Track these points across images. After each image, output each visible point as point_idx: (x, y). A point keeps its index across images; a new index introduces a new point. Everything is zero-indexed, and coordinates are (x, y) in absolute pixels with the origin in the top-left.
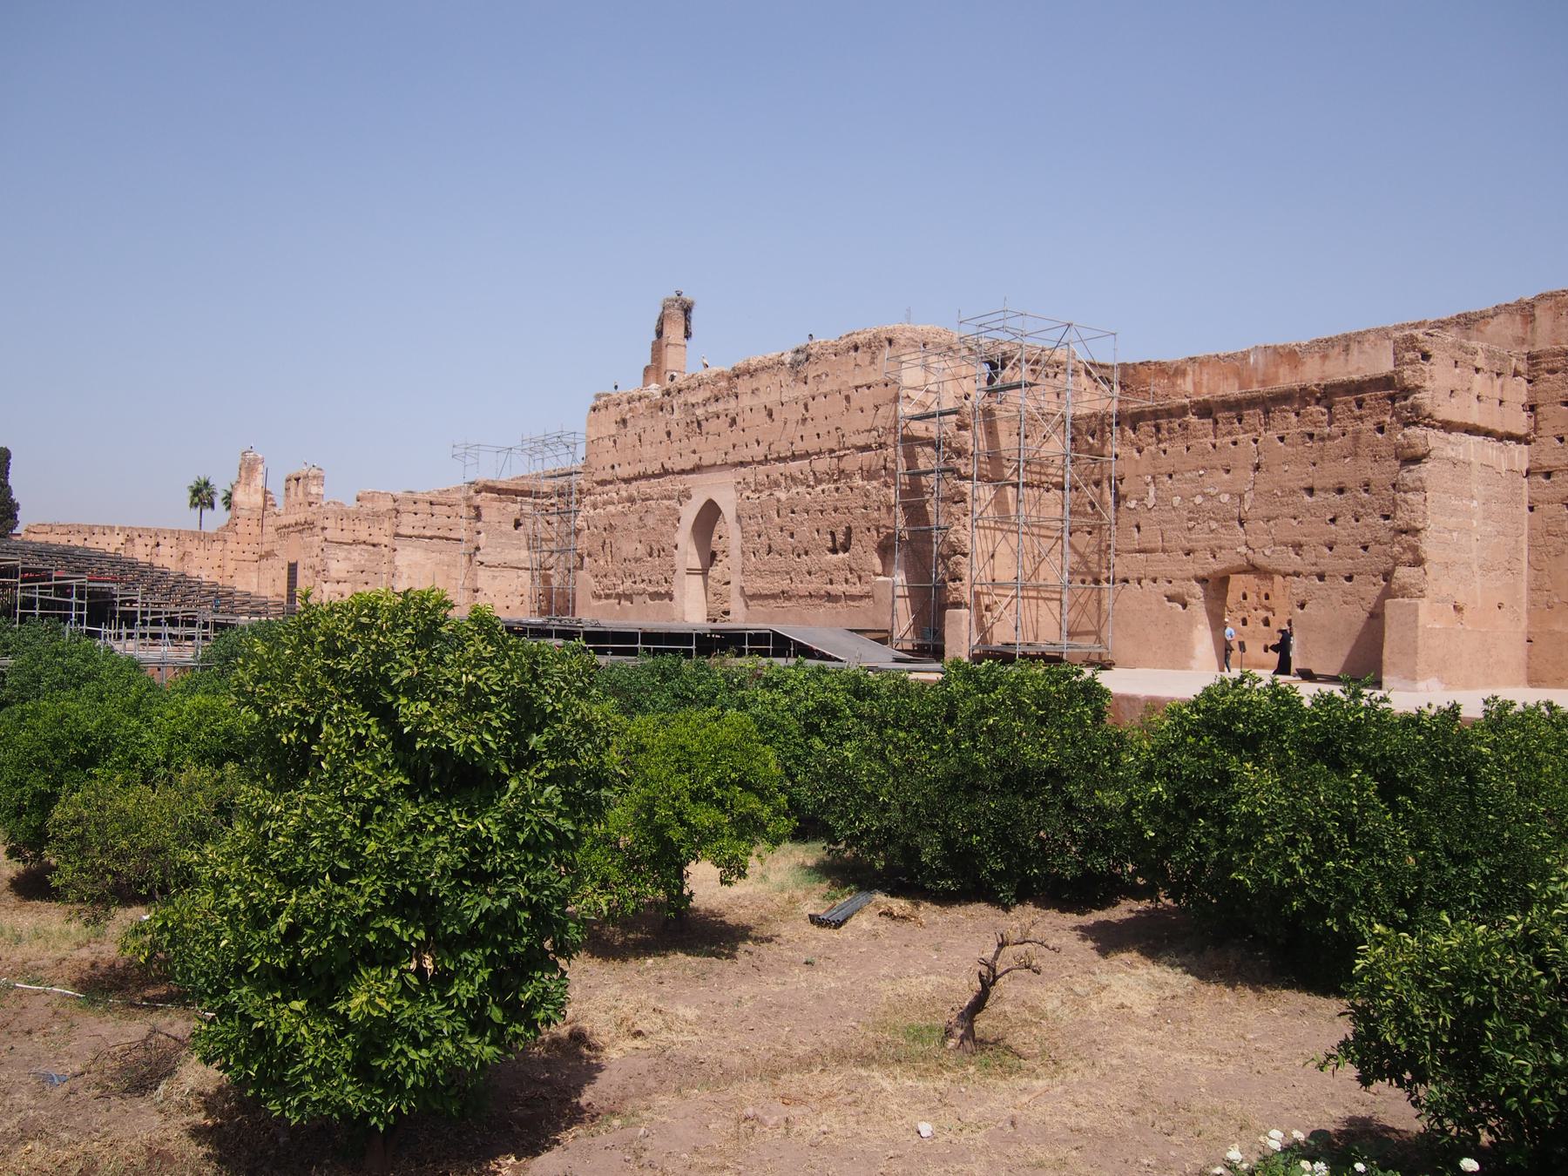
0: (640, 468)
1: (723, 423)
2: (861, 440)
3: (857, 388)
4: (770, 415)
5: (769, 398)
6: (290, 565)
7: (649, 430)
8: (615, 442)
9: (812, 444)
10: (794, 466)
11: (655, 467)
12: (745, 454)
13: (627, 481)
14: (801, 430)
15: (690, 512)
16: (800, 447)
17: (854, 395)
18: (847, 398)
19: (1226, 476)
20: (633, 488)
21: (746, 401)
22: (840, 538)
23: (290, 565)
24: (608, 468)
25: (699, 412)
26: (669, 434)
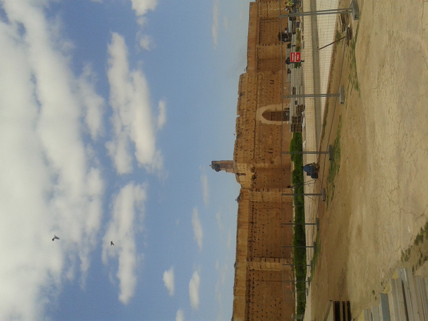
0: (253, 139)
2: (257, 79)
3: (248, 81)
5: (246, 100)
8: (245, 151)
10: (258, 94)
12: (255, 105)
13: (255, 144)
15: (264, 121)
16: (256, 93)
18: (249, 83)
19: (268, 39)
20: (257, 143)
22: (272, 82)
24: (251, 153)
25: (244, 120)
26: (247, 130)
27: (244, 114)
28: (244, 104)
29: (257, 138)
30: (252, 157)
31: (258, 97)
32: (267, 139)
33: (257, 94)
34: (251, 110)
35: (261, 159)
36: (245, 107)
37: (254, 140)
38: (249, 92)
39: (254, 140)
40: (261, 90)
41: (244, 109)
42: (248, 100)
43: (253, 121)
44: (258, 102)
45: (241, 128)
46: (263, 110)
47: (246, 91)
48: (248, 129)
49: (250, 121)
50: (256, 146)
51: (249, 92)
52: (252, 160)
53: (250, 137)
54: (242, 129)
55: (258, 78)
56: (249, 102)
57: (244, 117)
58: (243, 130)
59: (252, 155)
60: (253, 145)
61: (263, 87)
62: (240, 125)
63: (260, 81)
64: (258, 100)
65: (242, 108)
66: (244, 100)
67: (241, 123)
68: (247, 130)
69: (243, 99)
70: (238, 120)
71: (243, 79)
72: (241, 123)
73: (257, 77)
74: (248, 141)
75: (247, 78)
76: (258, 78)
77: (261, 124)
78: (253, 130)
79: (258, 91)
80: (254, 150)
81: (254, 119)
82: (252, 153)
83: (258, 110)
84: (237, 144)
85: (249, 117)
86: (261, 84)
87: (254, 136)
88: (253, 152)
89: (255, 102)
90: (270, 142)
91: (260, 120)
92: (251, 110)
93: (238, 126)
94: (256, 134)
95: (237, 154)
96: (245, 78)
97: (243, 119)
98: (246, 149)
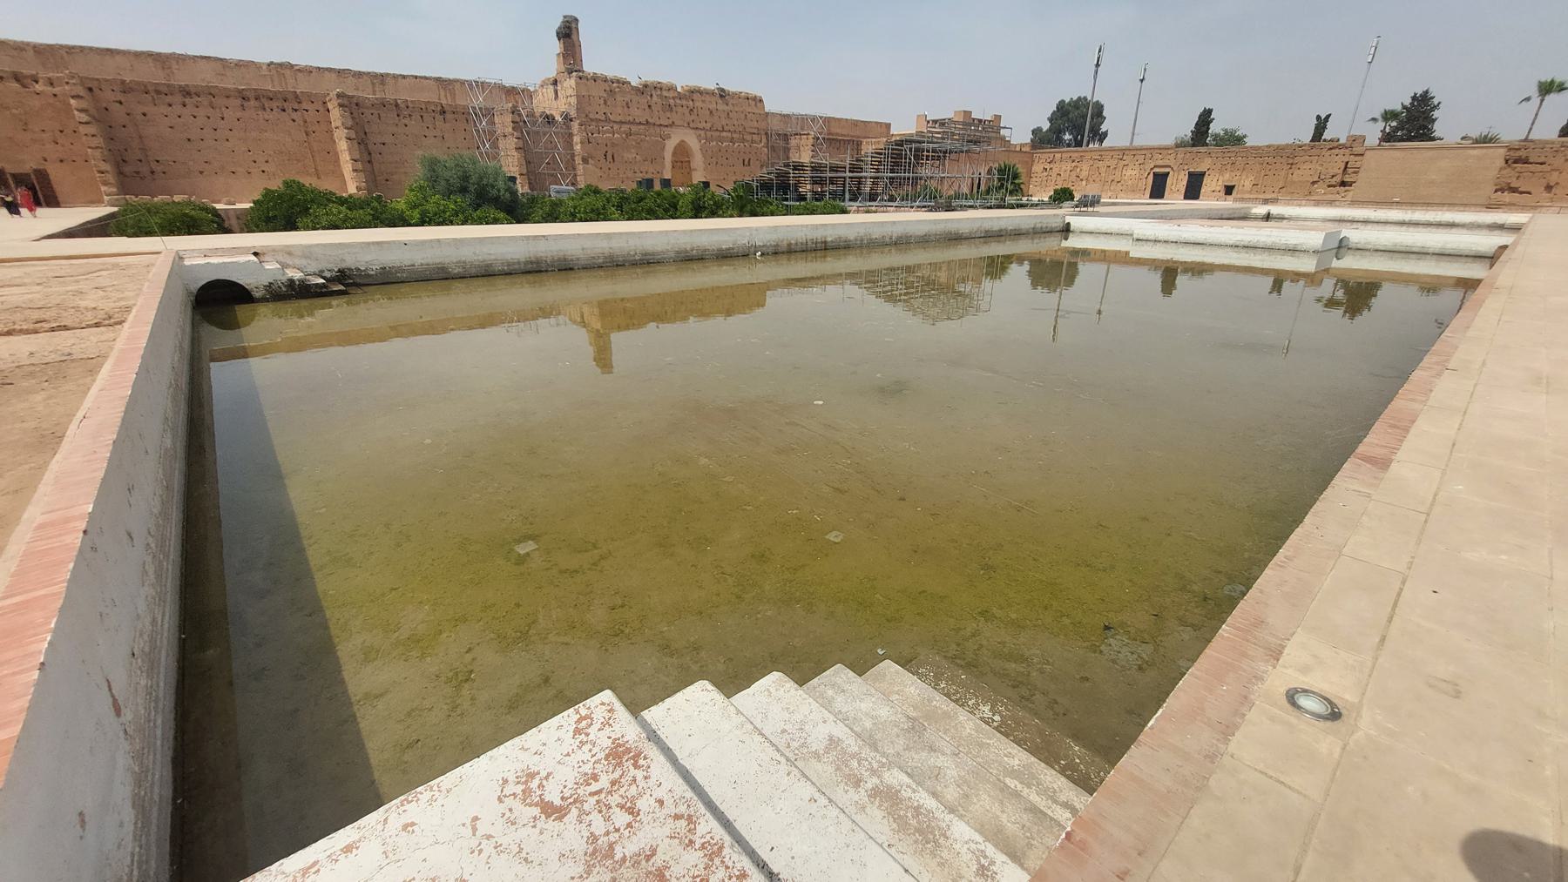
0: (631, 119)
1: (687, 112)
4: (711, 112)
5: (713, 106)
7: (634, 101)
10: (724, 134)
12: (700, 126)
13: (621, 122)
15: (671, 145)
20: (625, 128)
22: (746, 162)
27: (684, 102)
28: (703, 101)
29: (634, 128)
30: (591, 116)
31: (718, 133)
32: (633, 151)
33: (723, 131)
34: (693, 117)
35: (590, 134)
36: (699, 104)
37: (630, 123)
38: (728, 114)
39: (630, 123)
40: (732, 140)
41: (693, 100)
42: (711, 112)
44: (709, 133)
45: (653, 92)
46: (693, 143)
47: (730, 107)
48: (653, 108)
49: (668, 114)
50: (616, 127)
51: (728, 114)
52: (587, 116)
53: (638, 114)
54: (651, 95)
55: (754, 134)
56: (709, 112)
57: (678, 101)
58: (649, 98)
59: (597, 116)
60: (618, 119)
61: (737, 144)
62: (659, 93)
63: (748, 137)
65: (696, 96)
67: (665, 93)
68: (649, 106)
69: (713, 99)
70: (672, 88)
74: (626, 108)
75: (756, 111)
76: (754, 134)
77: (665, 138)
78: (650, 120)
79: (729, 134)
80: (607, 120)
81: (673, 123)
83: (692, 131)
84: (618, 81)
85: (677, 112)
86: (743, 140)
87: (637, 121)
88: (603, 118)
89: (709, 125)
90: (629, 156)
91: (672, 135)
92: (693, 117)
93: (658, 87)
94: (642, 127)
95: (595, 81)
96: (756, 105)
97: (673, 98)
98: (609, 103)
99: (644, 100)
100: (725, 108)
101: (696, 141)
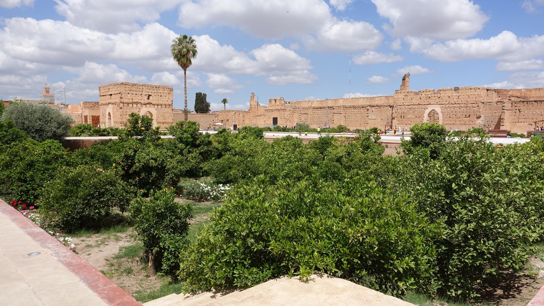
1: (437, 98)
6: (274, 118)
9: (461, 102)
11: (417, 104)
14: (457, 100)
15: (427, 112)
17: (470, 96)
20: (410, 107)
21: (442, 95)
23: (274, 118)
25: (430, 96)
27: (436, 95)
29: (413, 106)
30: (398, 104)
34: (439, 100)
36: (442, 95)
43: (429, 103)
44: (447, 106)
46: (438, 109)
47: (460, 94)
50: (407, 107)
53: (415, 101)
57: (433, 95)
58: (420, 95)
64: (449, 105)
66: (449, 94)
69: (451, 92)
71: (474, 90)
72: (427, 93)
73: (475, 102)
75: (475, 93)
82: (402, 104)
89: (447, 103)
90: (409, 116)
99: (418, 97)
100: (458, 94)
101: (440, 109)
